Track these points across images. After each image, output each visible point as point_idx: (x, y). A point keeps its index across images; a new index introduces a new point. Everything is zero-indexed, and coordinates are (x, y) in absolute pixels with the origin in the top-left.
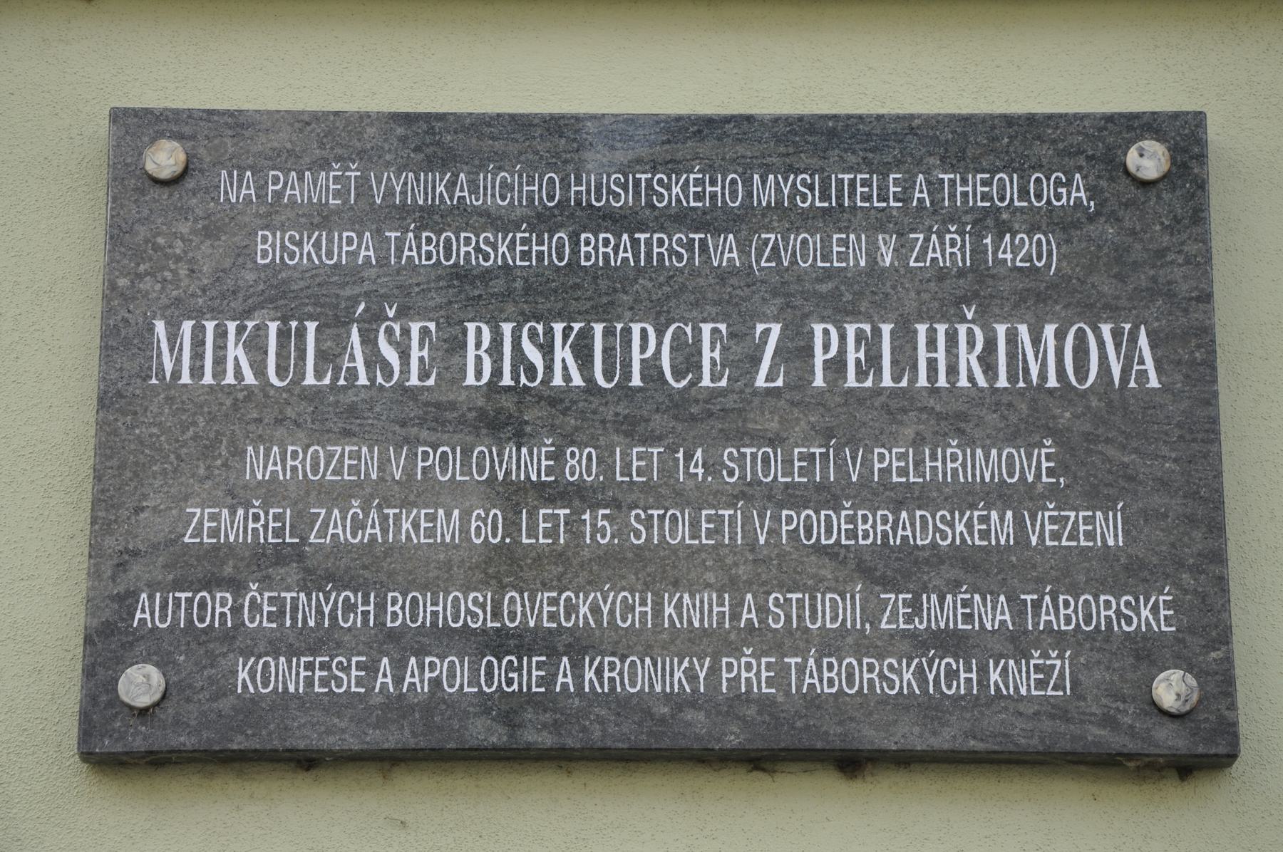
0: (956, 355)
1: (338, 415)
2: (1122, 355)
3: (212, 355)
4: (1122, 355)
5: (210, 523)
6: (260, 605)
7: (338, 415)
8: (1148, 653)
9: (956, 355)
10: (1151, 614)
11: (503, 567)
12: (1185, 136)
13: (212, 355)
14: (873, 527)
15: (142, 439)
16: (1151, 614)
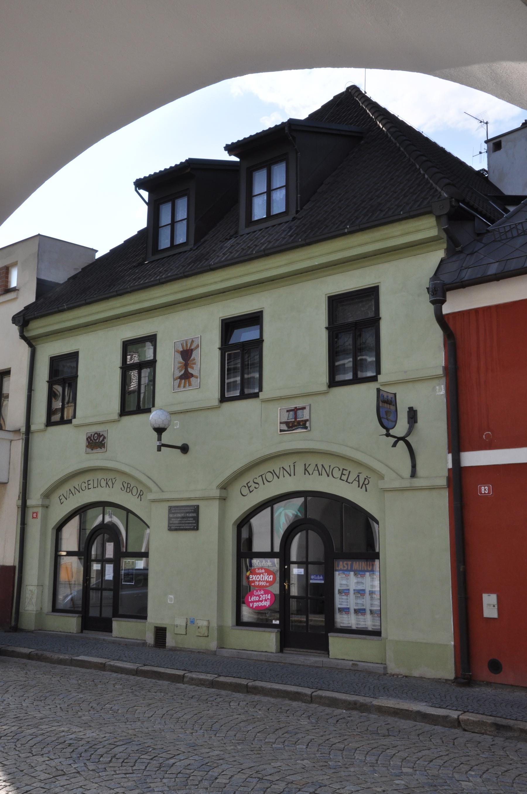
0: (191, 515)
1: (174, 518)
2: (194, 515)
3: (171, 516)
4: (194, 515)
5: (171, 522)
6: (172, 525)
7: (174, 518)
8: (194, 526)
9: (191, 515)
10: (195, 525)
11: (179, 523)
12: (198, 506)
13: (171, 516)
14: (188, 522)
15: (170, 519)
16: (195, 525)
